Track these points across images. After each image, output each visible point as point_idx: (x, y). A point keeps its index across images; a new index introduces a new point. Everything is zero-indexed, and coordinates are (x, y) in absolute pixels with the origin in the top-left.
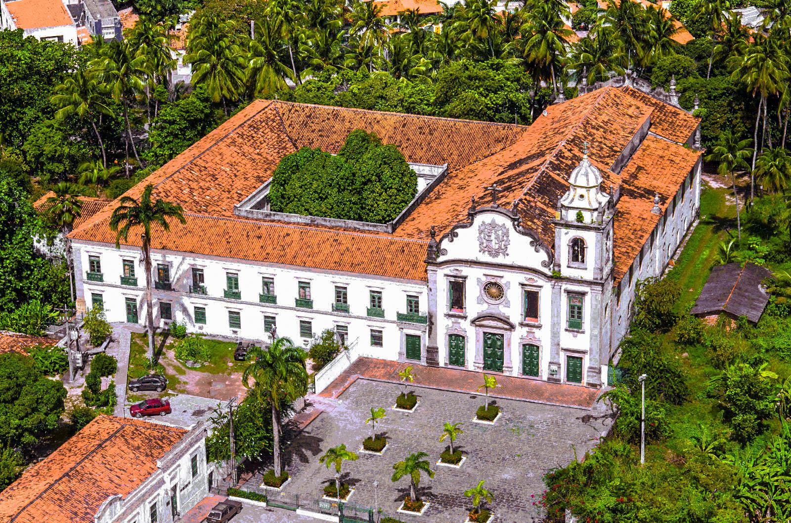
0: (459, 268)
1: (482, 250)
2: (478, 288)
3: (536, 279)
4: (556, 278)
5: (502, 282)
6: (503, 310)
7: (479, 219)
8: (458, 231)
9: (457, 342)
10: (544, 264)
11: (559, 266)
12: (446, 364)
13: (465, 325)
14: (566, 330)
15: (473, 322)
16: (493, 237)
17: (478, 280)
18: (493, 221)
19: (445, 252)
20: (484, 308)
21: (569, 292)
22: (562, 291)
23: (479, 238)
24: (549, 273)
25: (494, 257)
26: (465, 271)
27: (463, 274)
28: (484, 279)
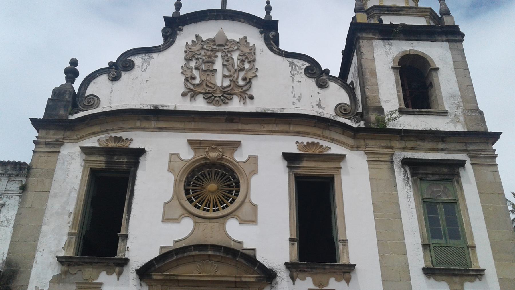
0: (124, 135)
1: (191, 93)
2: (171, 178)
3: (324, 143)
5: (240, 157)
6: (236, 232)
8: (137, 60)
10: (341, 109)
11: (380, 110)
14: (428, 272)
16: (218, 65)
17: (174, 156)
18: (221, 34)
19: (94, 101)
20: (182, 231)
21: (412, 166)
24: (362, 124)
25: (217, 104)
27: (133, 145)
28: (188, 155)
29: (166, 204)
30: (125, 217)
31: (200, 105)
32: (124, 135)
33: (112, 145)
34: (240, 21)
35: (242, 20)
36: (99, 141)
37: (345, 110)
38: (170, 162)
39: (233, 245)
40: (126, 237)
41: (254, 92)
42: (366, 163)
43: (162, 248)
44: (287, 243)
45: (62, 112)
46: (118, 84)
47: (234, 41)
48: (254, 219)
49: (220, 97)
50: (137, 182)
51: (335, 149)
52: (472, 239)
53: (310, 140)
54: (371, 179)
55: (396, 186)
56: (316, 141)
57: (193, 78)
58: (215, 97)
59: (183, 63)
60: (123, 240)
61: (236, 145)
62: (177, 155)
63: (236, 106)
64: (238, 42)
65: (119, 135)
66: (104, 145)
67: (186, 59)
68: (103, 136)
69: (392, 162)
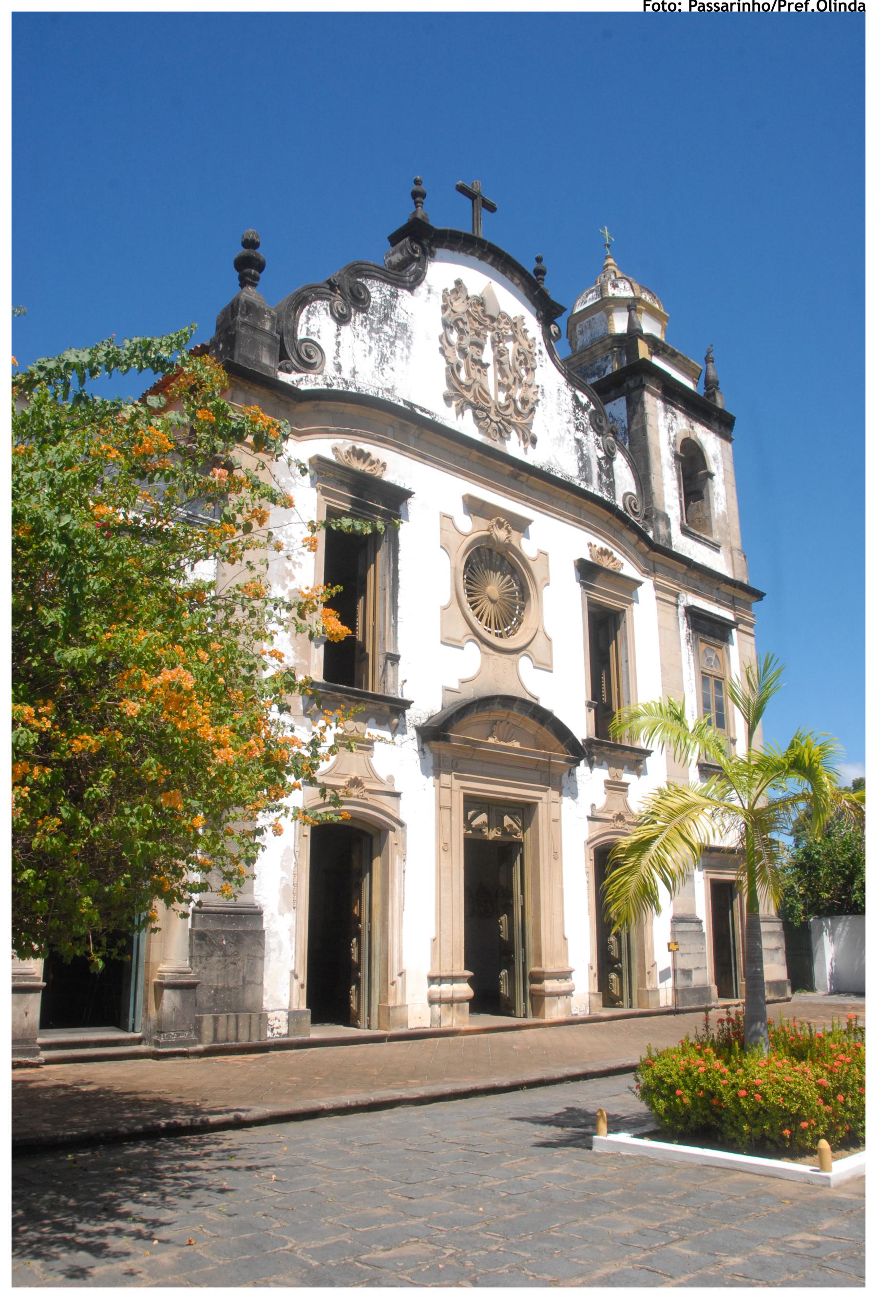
4: (659, 557)
5: (528, 547)
7: (442, 272)
9: (346, 856)
12: (293, 1016)
13: (396, 760)
15: (434, 734)
22: (681, 610)
23: (444, 339)
26: (398, 467)
29: (444, 609)
30: (390, 621)
31: (466, 425)
32: (378, 452)
33: (358, 466)
34: (512, 280)
35: (517, 281)
36: (335, 450)
37: (635, 506)
38: (441, 529)
39: (528, 698)
40: (394, 659)
41: (536, 430)
42: (654, 602)
43: (447, 690)
44: (584, 708)
45: (266, 360)
46: (346, 330)
47: (509, 318)
48: (549, 663)
49: (497, 423)
50: (400, 555)
51: (629, 570)
52: (734, 731)
53: (605, 546)
54: (660, 627)
55: (680, 643)
56: (610, 549)
57: (459, 368)
58: (491, 420)
59: (441, 330)
60: (393, 665)
61: (521, 525)
62: (451, 518)
63: (513, 447)
64: (515, 324)
65: (366, 448)
66: (344, 462)
67: (446, 325)
68: (340, 441)
69: (677, 606)
